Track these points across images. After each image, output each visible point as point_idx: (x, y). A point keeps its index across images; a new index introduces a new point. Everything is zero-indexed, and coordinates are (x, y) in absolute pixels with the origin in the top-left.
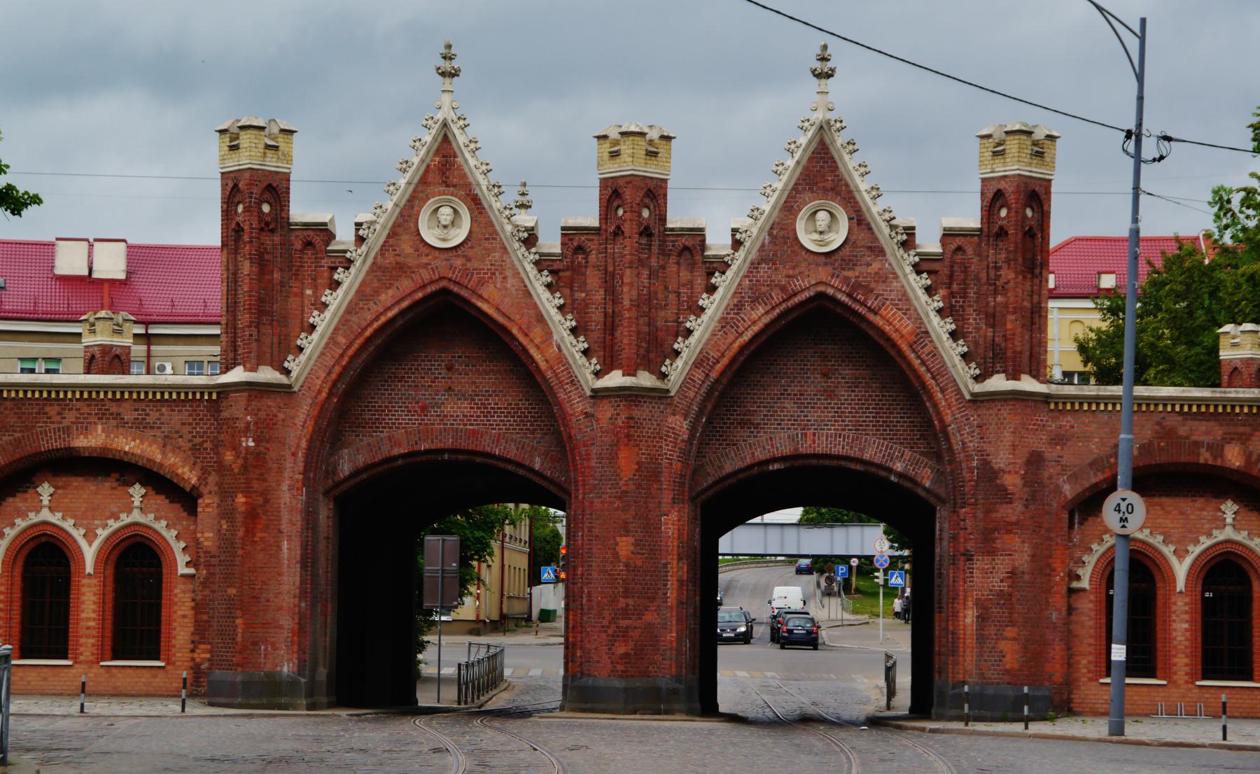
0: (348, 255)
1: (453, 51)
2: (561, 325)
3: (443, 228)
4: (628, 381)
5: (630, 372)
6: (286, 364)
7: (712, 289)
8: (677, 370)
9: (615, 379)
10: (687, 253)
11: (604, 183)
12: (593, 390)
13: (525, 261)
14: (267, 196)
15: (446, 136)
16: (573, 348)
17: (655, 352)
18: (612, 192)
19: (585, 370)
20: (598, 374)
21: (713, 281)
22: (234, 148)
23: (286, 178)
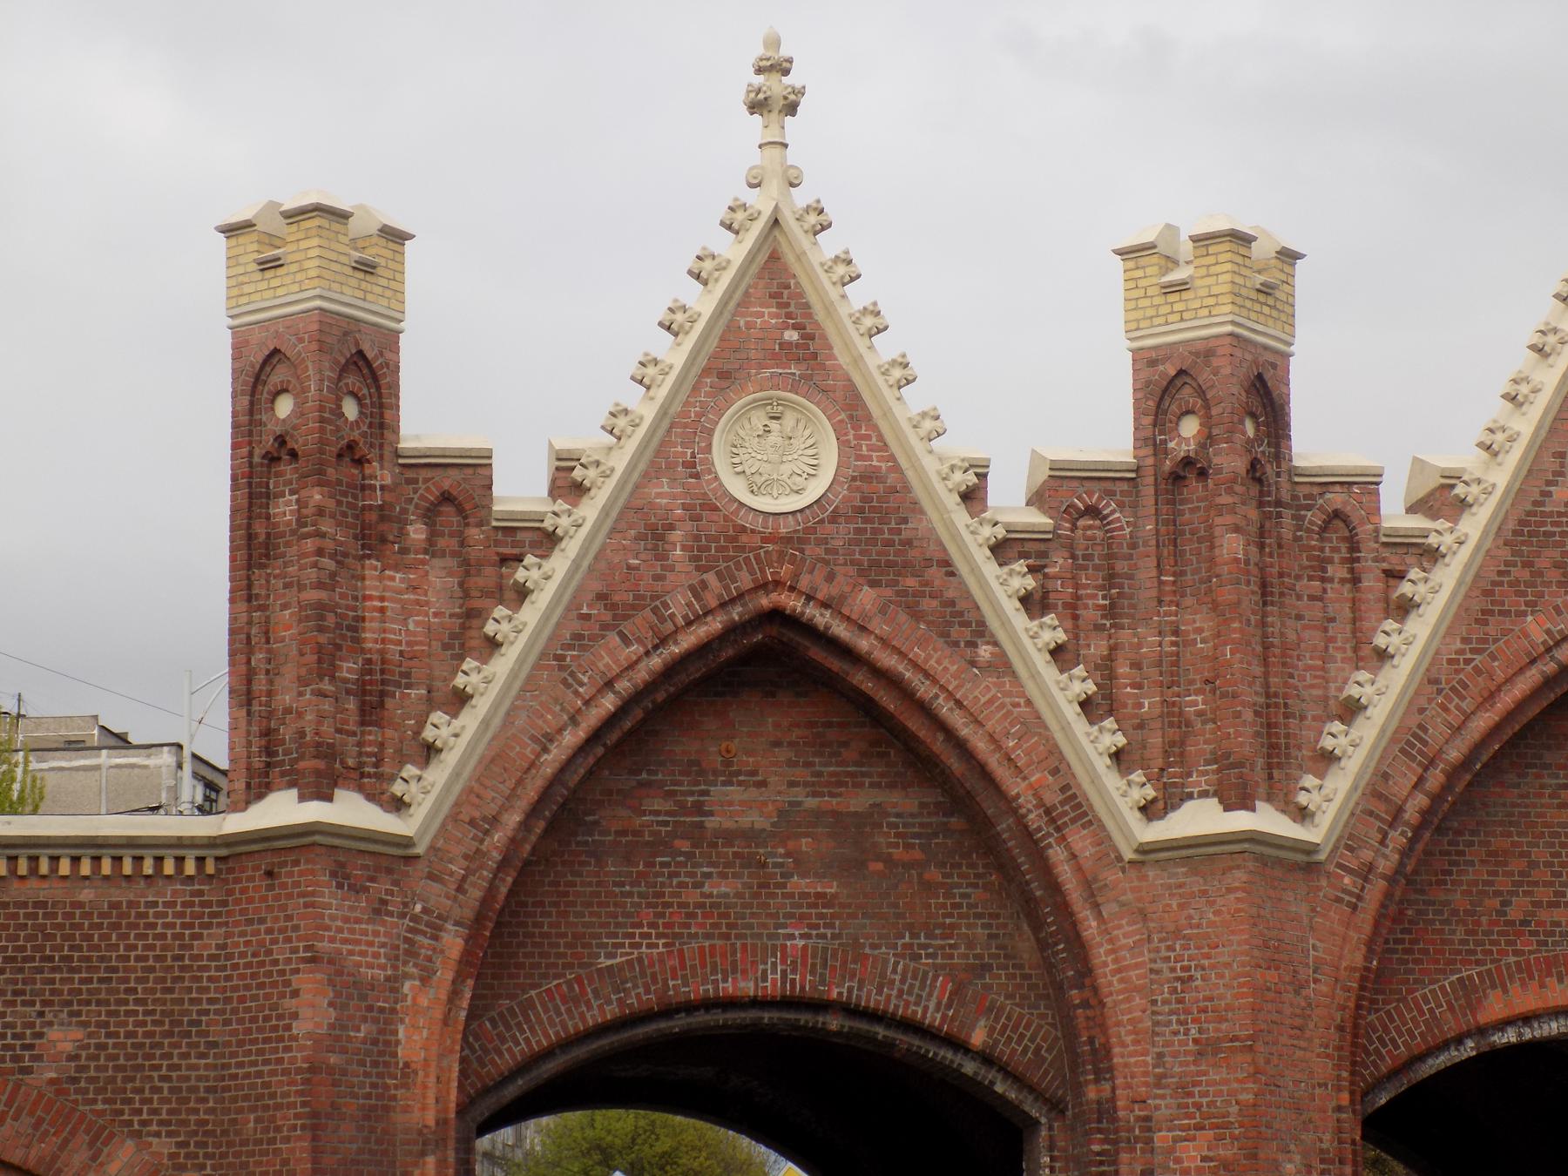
0: (548, 524)
1: (784, 52)
2: (1061, 693)
3: (779, 469)
4: (1240, 821)
5: (1237, 798)
6: (398, 788)
7: (1404, 608)
8: (1330, 798)
9: (1201, 818)
10: (1338, 523)
11: (1145, 360)
12: (1145, 850)
13: (968, 540)
14: (351, 380)
15: (775, 257)
16: (1091, 746)
17: (1270, 760)
18: (1166, 387)
19: (1119, 797)
20: (1148, 810)
21: (1406, 588)
22: (269, 265)
23: (391, 340)
